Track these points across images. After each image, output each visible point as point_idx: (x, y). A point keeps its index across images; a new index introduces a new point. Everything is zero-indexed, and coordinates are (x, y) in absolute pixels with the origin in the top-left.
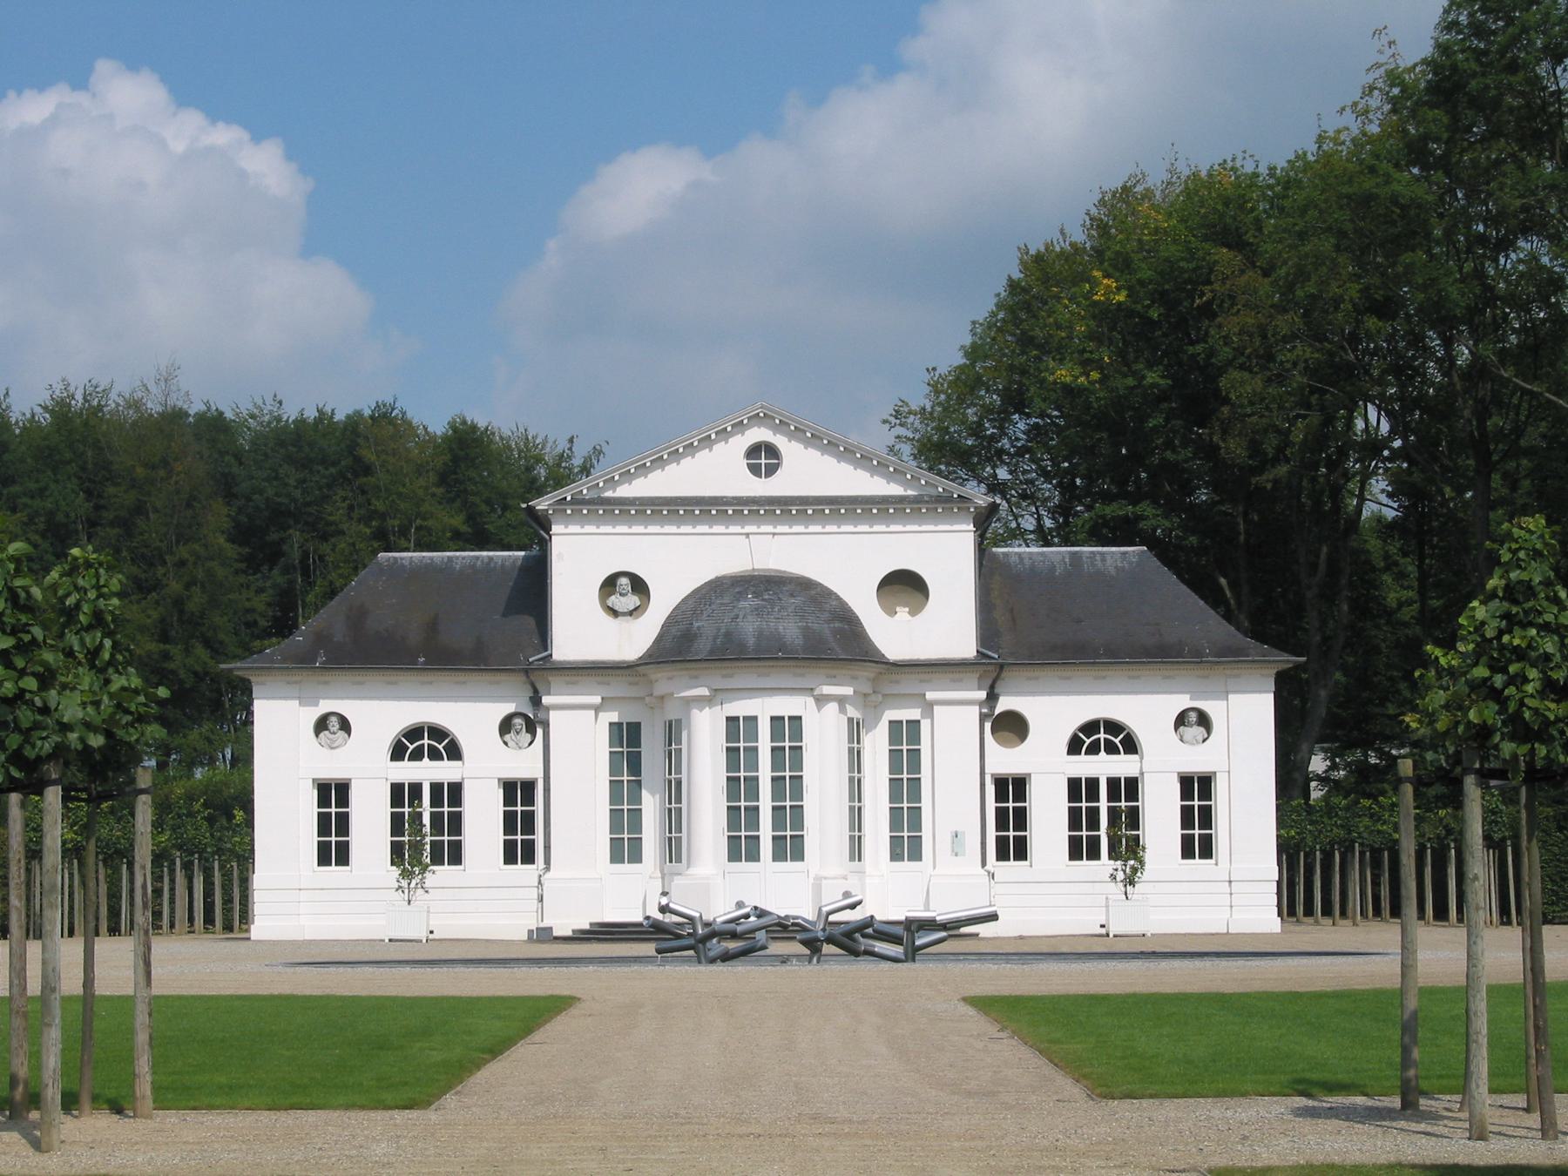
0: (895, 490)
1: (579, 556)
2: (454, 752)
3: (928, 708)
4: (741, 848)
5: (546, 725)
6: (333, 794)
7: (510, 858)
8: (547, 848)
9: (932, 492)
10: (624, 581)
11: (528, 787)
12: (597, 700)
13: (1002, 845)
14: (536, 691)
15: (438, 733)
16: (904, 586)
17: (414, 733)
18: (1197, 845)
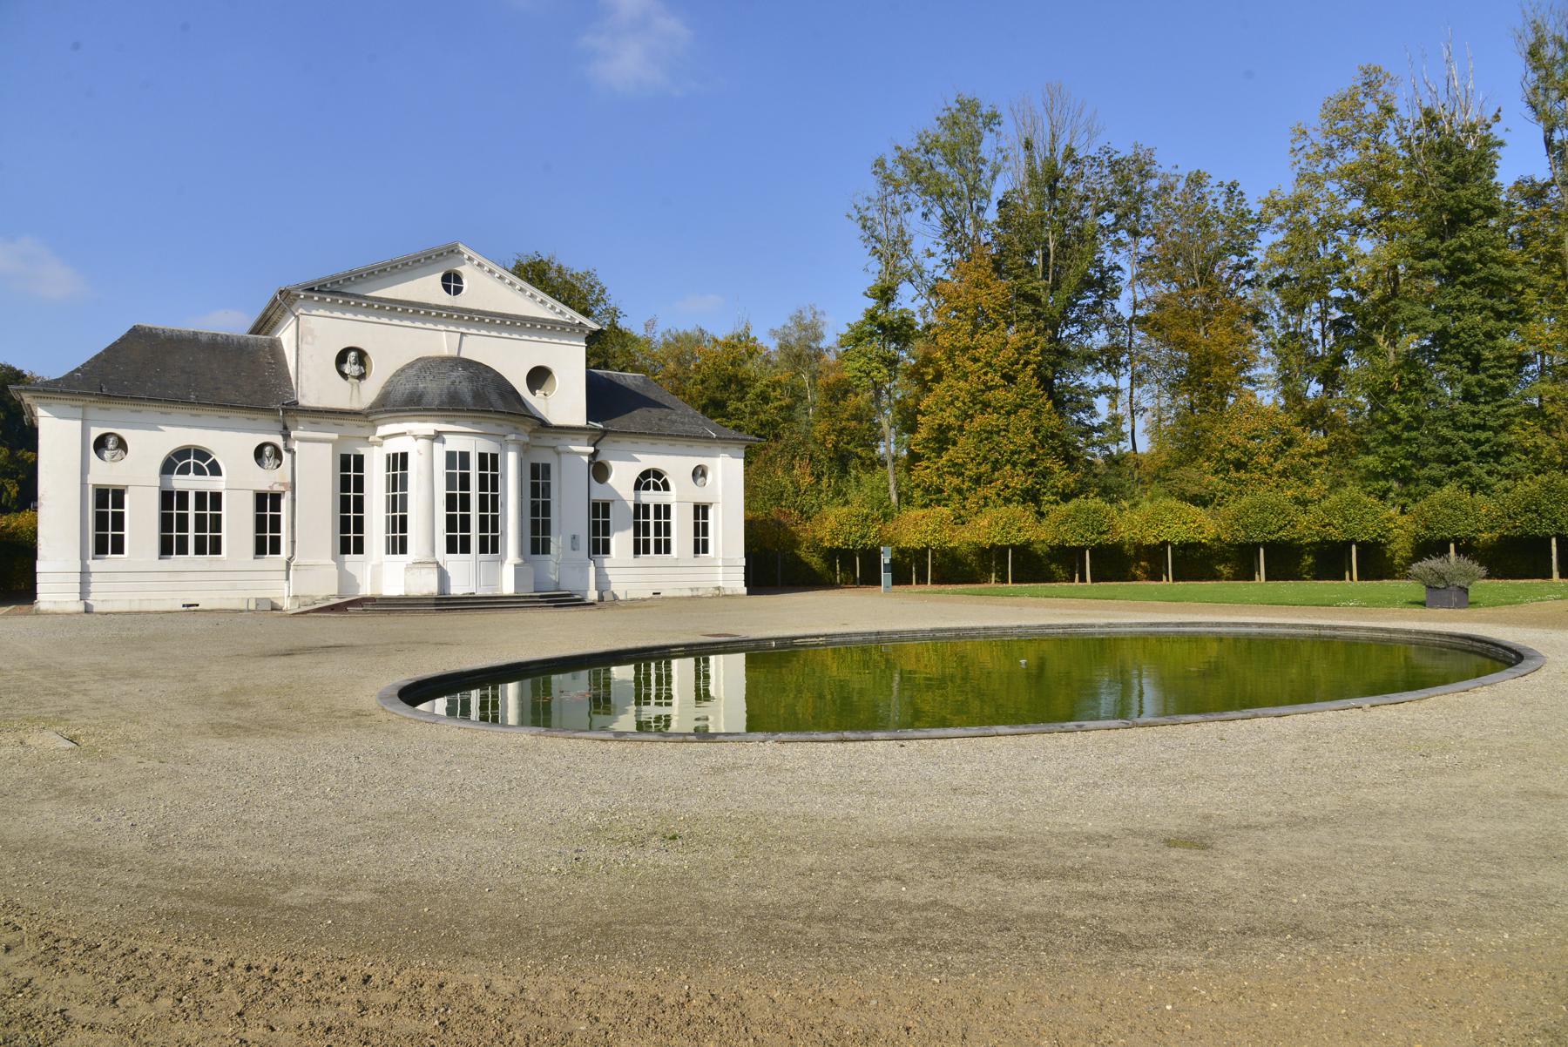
2: (215, 470)
5: (291, 451)
8: (293, 542)
11: (276, 498)
12: (335, 436)
13: (596, 542)
14: (285, 428)
15: (202, 454)
18: (701, 547)
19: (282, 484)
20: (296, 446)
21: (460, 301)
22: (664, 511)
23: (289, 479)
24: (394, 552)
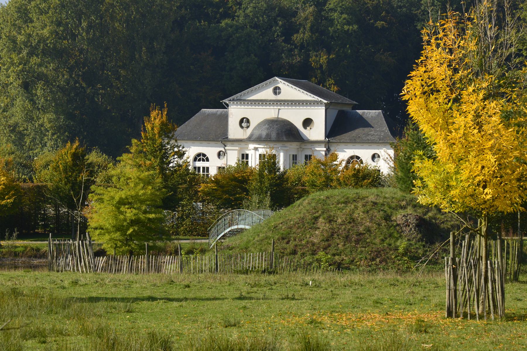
2: (208, 160)
20: (228, 151)
21: (279, 97)
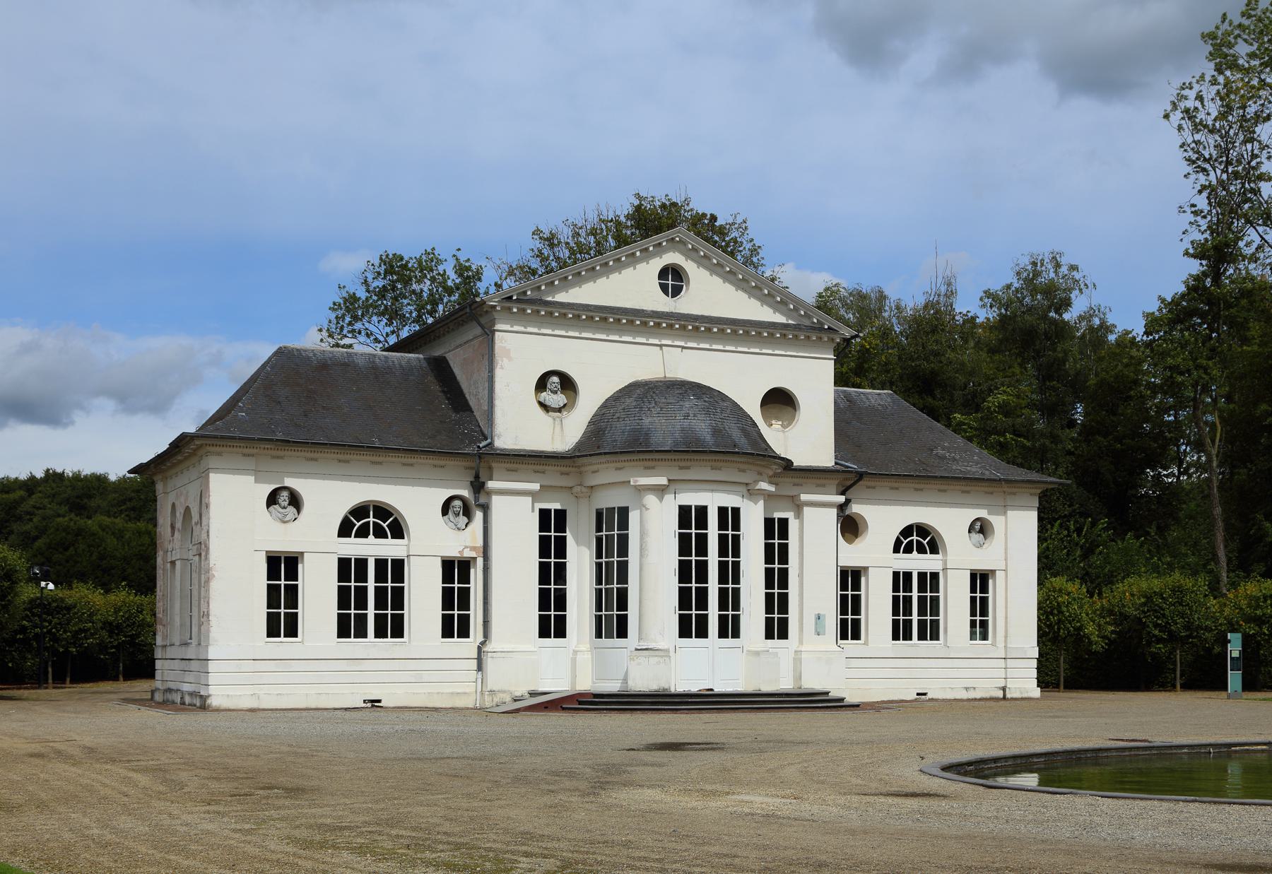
0: (779, 318)
1: (521, 353)
2: (398, 531)
3: (798, 508)
4: (691, 627)
5: (485, 508)
6: (283, 567)
7: (447, 632)
9: (807, 323)
10: (555, 379)
12: (536, 487)
14: (477, 477)
15: (383, 511)
16: (780, 401)
17: (360, 511)
18: (980, 629)
19: (473, 549)
22: (930, 581)
23: (480, 543)
24: (609, 636)
